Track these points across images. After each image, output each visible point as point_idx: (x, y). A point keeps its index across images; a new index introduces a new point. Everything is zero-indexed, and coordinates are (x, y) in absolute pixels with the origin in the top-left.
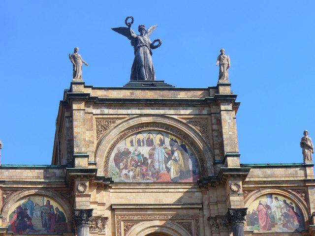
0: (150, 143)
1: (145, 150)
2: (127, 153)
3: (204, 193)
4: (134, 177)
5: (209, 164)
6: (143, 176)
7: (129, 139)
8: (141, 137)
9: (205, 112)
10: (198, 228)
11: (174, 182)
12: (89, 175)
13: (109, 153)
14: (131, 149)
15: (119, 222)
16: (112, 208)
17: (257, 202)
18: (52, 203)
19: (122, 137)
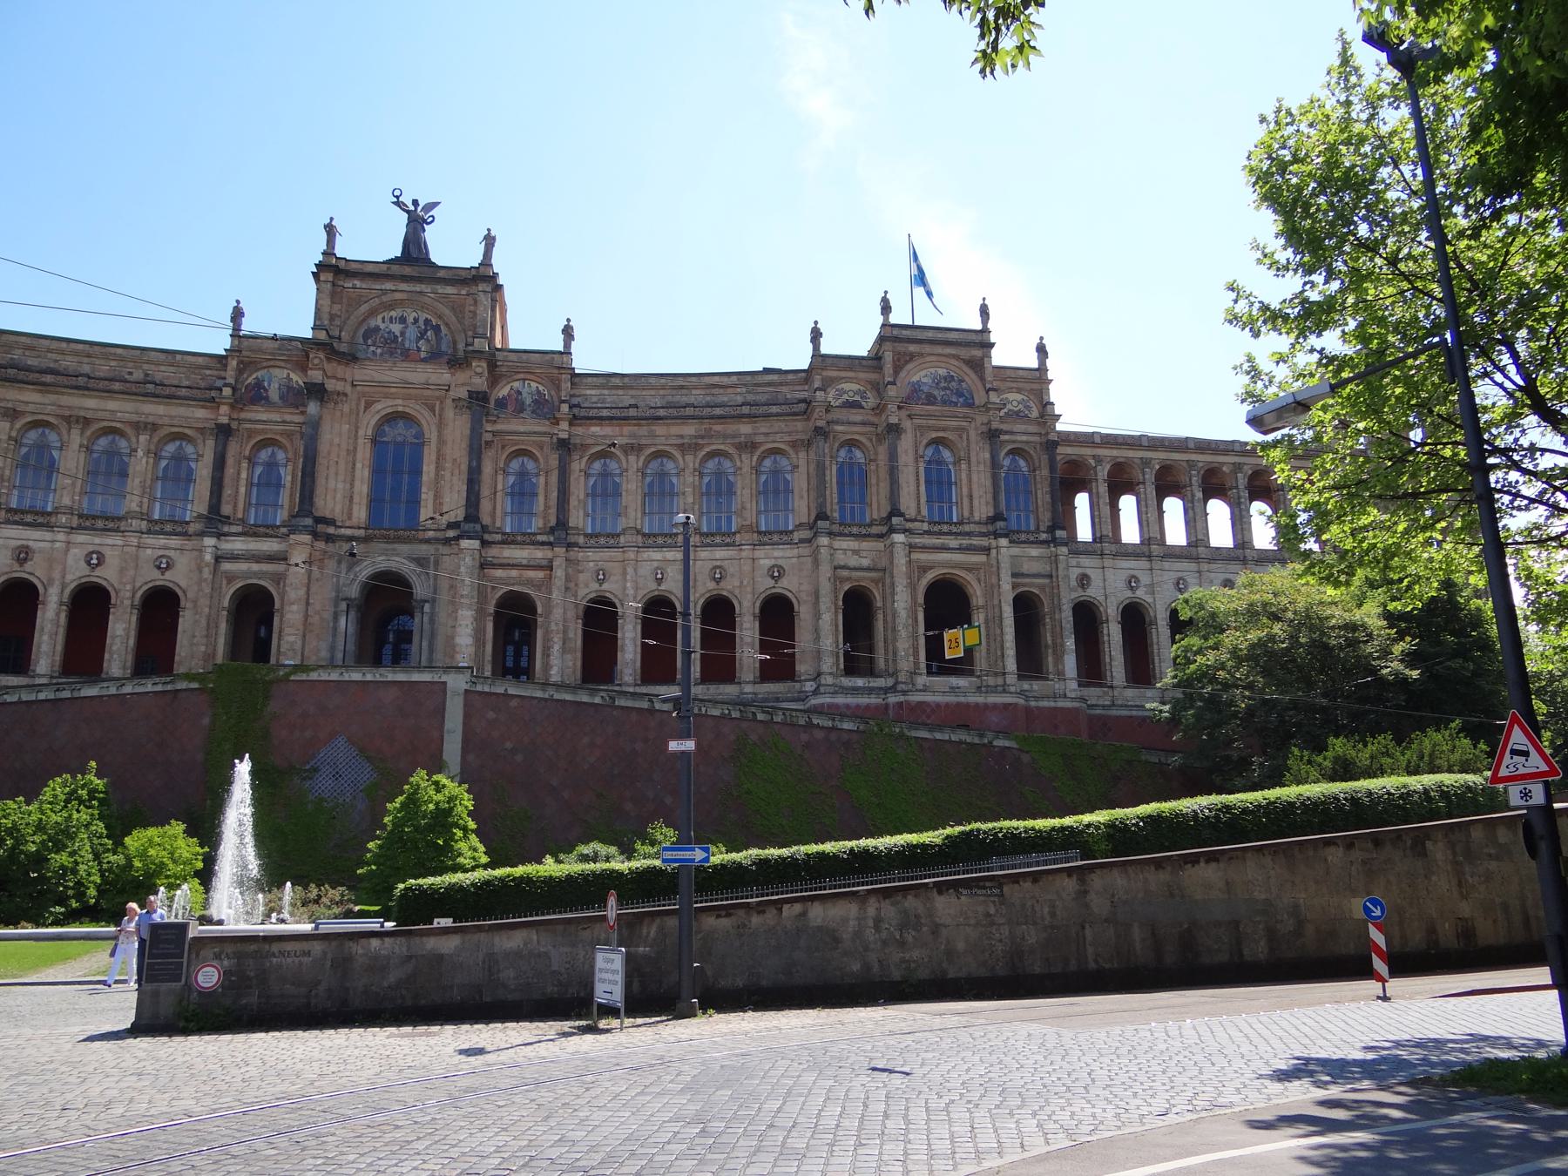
0: (403, 320)
1: (396, 328)
2: (377, 329)
3: (453, 374)
4: (381, 354)
5: (461, 346)
6: (391, 354)
7: (380, 317)
8: (393, 314)
9: (464, 292)
10: (442, 409)
11: (424, 360)
13: (357, 329)
14: (382, 326)
15: (359, 399)
16: (353, 386)
17: (508, 387)
18: (293, 376)
19: (373, 313)
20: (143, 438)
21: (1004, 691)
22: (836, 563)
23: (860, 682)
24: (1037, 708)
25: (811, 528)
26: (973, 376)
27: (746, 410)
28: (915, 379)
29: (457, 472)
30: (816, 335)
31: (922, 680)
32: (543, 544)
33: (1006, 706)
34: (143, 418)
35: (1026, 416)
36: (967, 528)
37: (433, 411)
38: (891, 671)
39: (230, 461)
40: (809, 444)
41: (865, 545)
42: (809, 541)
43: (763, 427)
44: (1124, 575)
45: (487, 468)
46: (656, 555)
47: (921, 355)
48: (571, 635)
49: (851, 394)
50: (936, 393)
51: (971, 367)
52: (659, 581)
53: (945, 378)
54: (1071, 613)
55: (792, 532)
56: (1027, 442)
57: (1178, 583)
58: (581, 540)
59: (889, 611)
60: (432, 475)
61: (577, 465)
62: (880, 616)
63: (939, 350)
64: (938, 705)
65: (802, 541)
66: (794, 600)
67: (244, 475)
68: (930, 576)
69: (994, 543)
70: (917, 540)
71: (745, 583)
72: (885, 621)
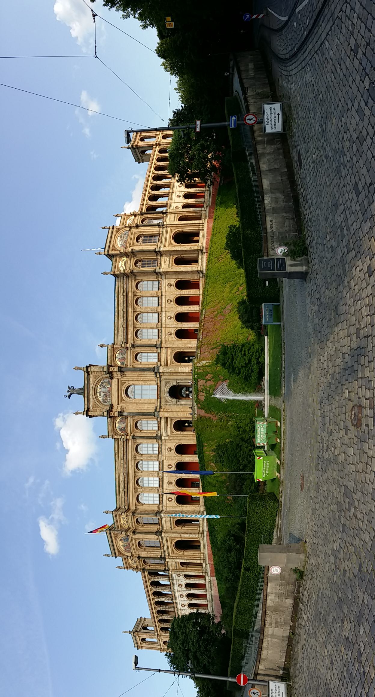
12: (109, 411)
20: (138, 458)
29: (141, 375)
32: (161, 350)
34: (133, 459)
36: (161, 232)
37: (125, 383)
39: (141, 435)
42: (161, 275)
45: (140, 366)
46: (164, 318)
48: (186, 342)
52: (171, 318)
58: (160, 340)
60: (142, 382)
61: (138, 342)
65: (161, 278)
67: (145, 432)
68: (173, 242)
70: (163, 246)
71: (172, 294)
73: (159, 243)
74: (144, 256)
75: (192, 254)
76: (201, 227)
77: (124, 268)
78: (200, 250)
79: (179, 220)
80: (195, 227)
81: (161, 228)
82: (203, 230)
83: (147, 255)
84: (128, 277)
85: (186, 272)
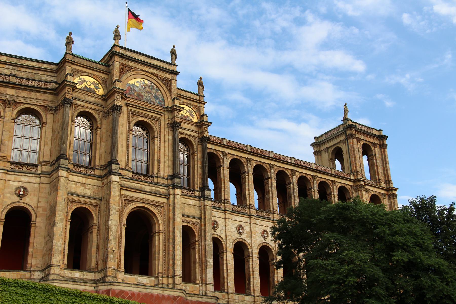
21: (173, 288)
22: (69, 190)
23: (77, 274)
24: (191, 301)
25: (51, 166)
26: (165, 89)
27: (12, 79)
28: (131, 82)
30: (70, 42)
31: (122, 276)
33: (175, 298)
35: (191, 120)
38: (100, 268)
40: (56, 110)
41: (89, 181)
42: (49, 174)
43: (24, 94)
44: (237, 224)
47: (137, 69)
49: (89, 83)
50: (143, 94)
51: (164, 83)
53: (149, 86)
54: (212, 243)
55: (36, 166)
56: (190, 136)
57: (263, 233)
59: (102, 227)
62: (95, 230)
63: (147, 69)
64: (133, 294)
65: (43, 173)
66: (33, 213)
68: (132, 206)
69: (171, 192)
70: (126, 183)
72: (98, 234)
73: (131, 175)
74: (104, 137)
75: (97, 254)
76: (165, 281)
77: (79, 87)
78: (106, 276)
79: (183, 227)
80: (166, 266)
81: (166, 182)
82: (156, 285)
83: (103, 144)
84: (56, 92)
85: (50, 236)
